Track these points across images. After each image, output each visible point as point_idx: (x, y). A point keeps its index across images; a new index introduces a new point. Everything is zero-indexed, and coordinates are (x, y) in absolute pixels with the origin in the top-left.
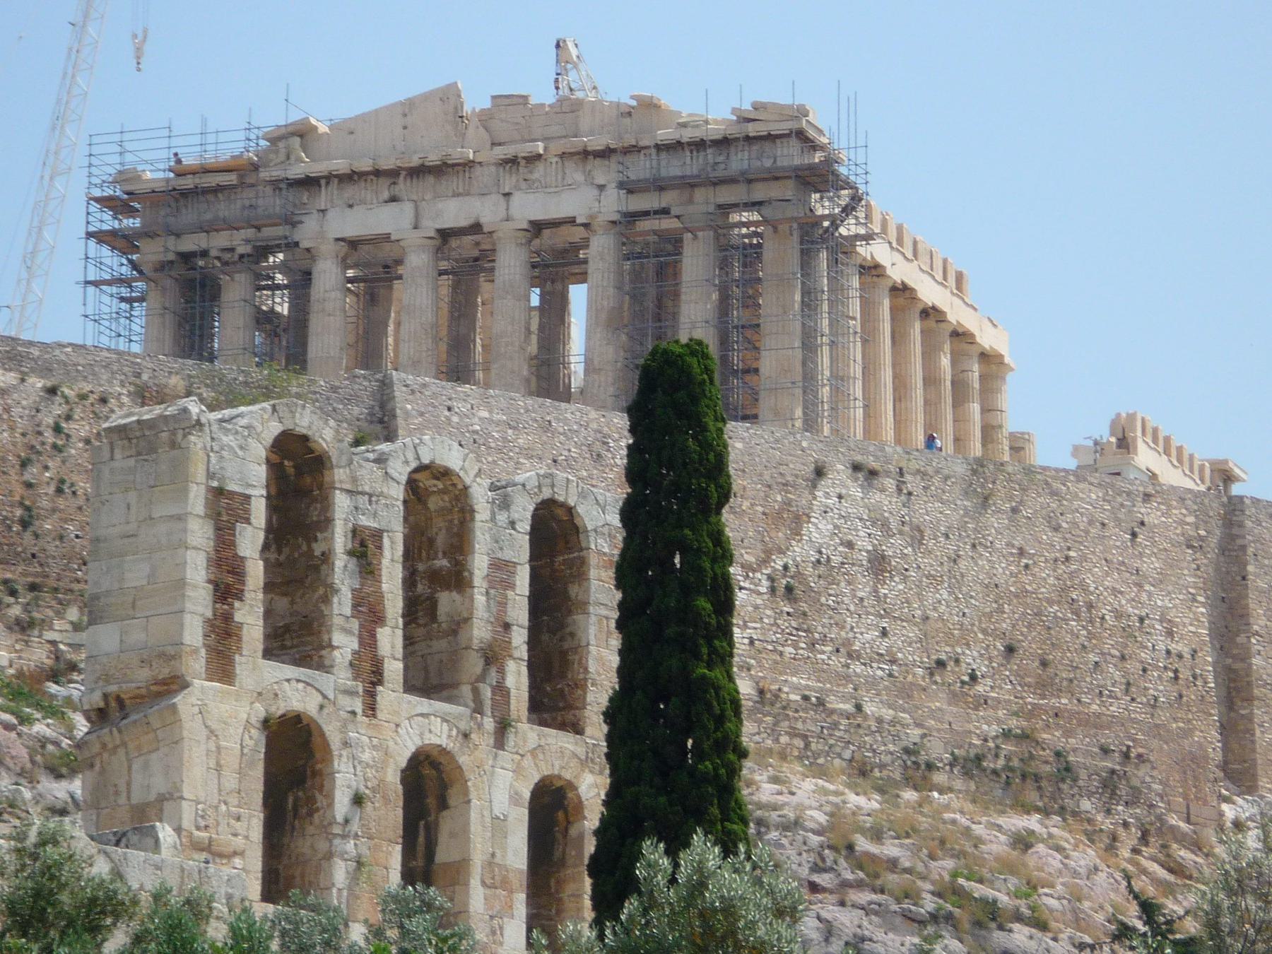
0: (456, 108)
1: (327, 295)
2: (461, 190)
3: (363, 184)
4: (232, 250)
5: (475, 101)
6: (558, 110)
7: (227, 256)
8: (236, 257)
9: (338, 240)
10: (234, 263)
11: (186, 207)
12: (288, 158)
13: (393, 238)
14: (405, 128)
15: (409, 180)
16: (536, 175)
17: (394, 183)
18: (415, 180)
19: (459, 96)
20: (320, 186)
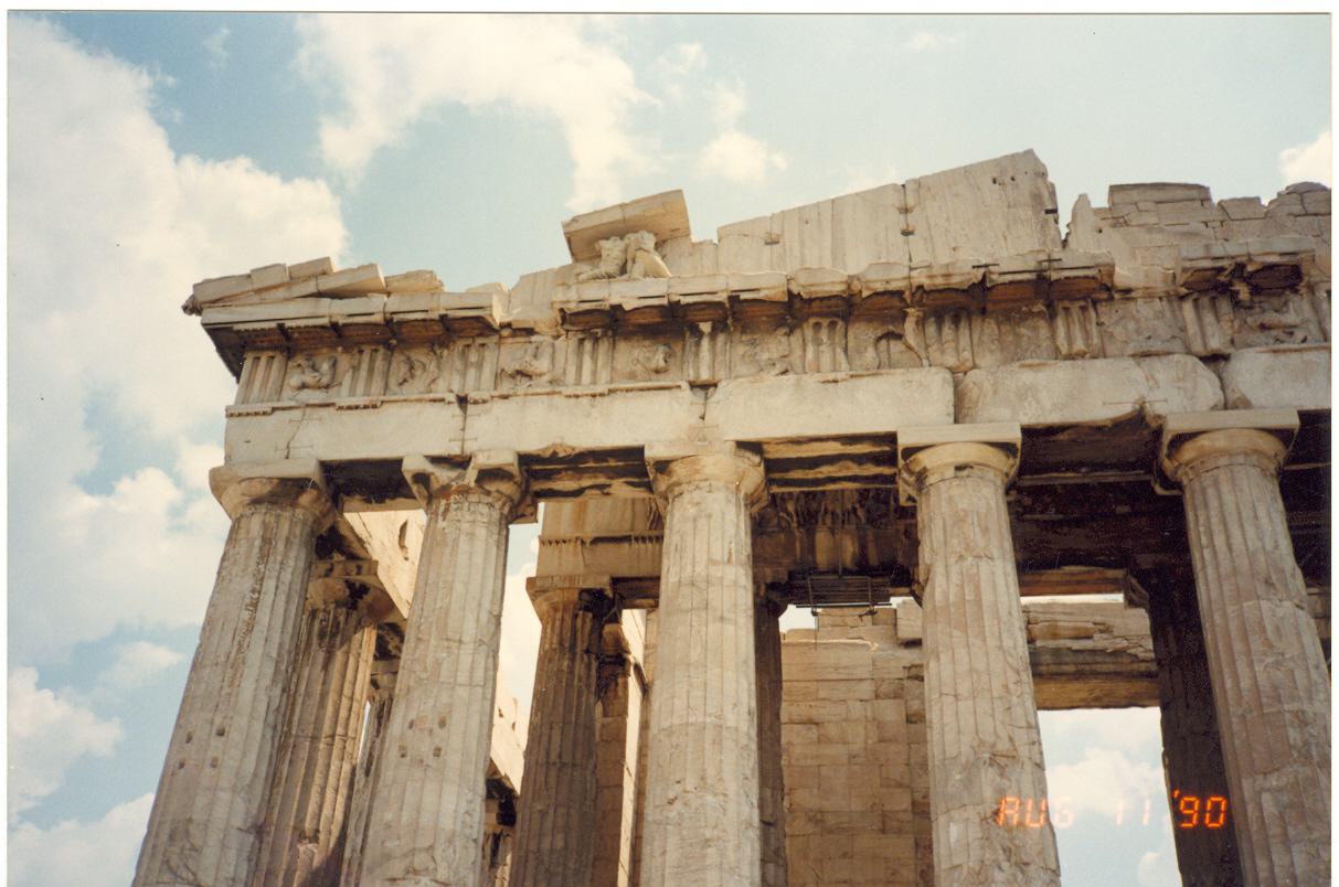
0: (1037, 197)
1: (716, 572)
2: (1079, 345)
3: (809, 332)
4: (460, 463)
5: (1081, 181)
6: (1297, 209)
7: (443, 475)
8: (471, 475)
9: (744, 446)
10: (465, 491)
11: (356, 369)
12: (623, 270)
13: (904, 441)
14: (906, 233)
15: (931, 329)
16: (1290, 318)
17: (889, 336)
18: (947, 330)
19: (1044, 175)
20: (700, 335)
